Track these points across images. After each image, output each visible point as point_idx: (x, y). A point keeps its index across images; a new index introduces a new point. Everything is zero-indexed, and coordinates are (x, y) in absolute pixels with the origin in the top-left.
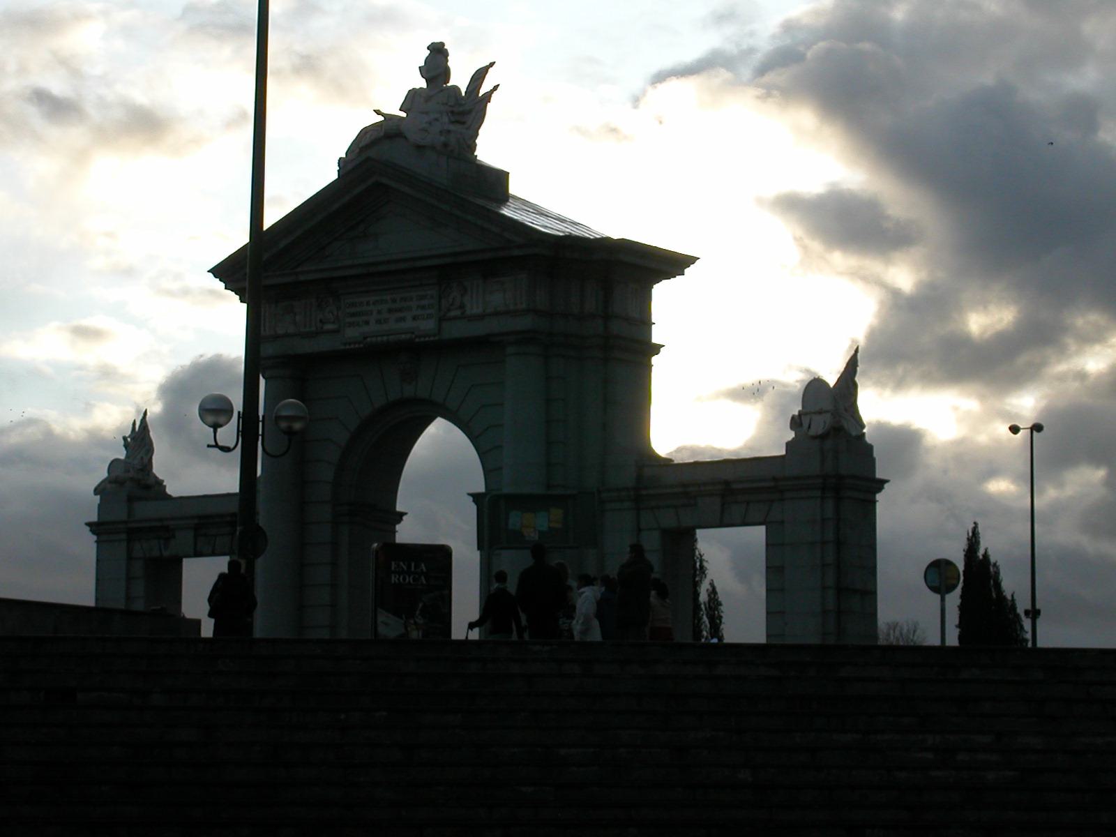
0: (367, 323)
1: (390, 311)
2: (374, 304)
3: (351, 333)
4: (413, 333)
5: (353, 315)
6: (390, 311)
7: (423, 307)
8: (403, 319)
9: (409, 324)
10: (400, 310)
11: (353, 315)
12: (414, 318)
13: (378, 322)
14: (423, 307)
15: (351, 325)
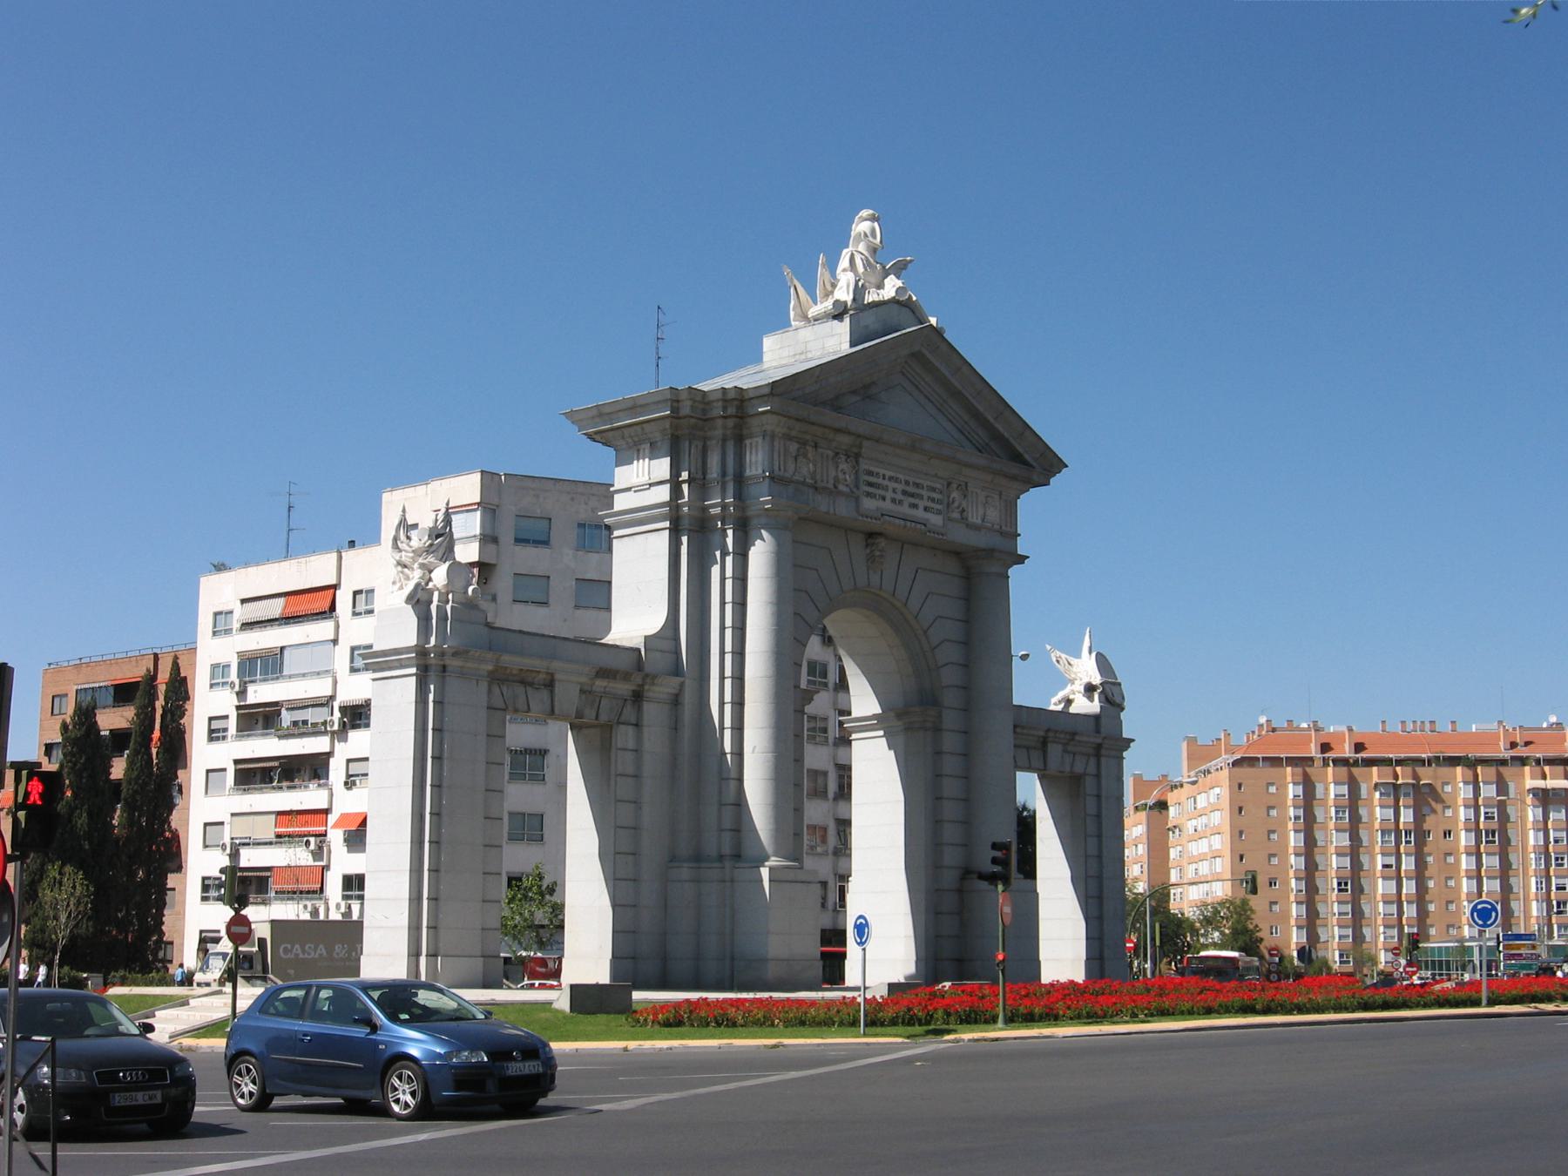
0: (884, 499)
1: (905, 493)
2: (891, 478)
3: (869, 504)
4: (925, 525)
5: (870, 484)
6: (905, 493)
7: (933, 500)
8: (915, 506)
9: (919, 513)
10: (912, 495)
11: (870, 484)
12: (926, 509)
13: (893, 501)
14: (933, 500)
15: (868, 494)
